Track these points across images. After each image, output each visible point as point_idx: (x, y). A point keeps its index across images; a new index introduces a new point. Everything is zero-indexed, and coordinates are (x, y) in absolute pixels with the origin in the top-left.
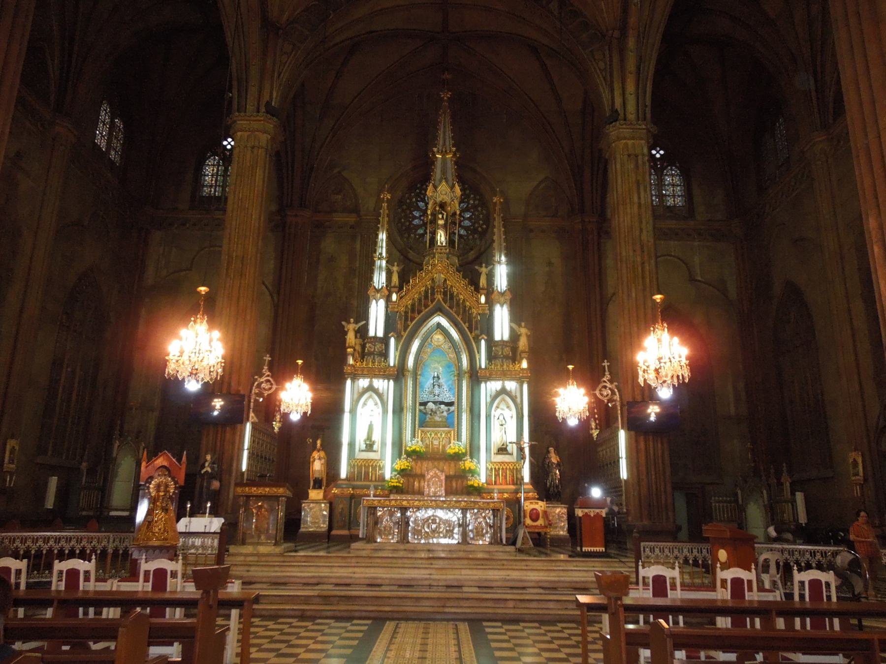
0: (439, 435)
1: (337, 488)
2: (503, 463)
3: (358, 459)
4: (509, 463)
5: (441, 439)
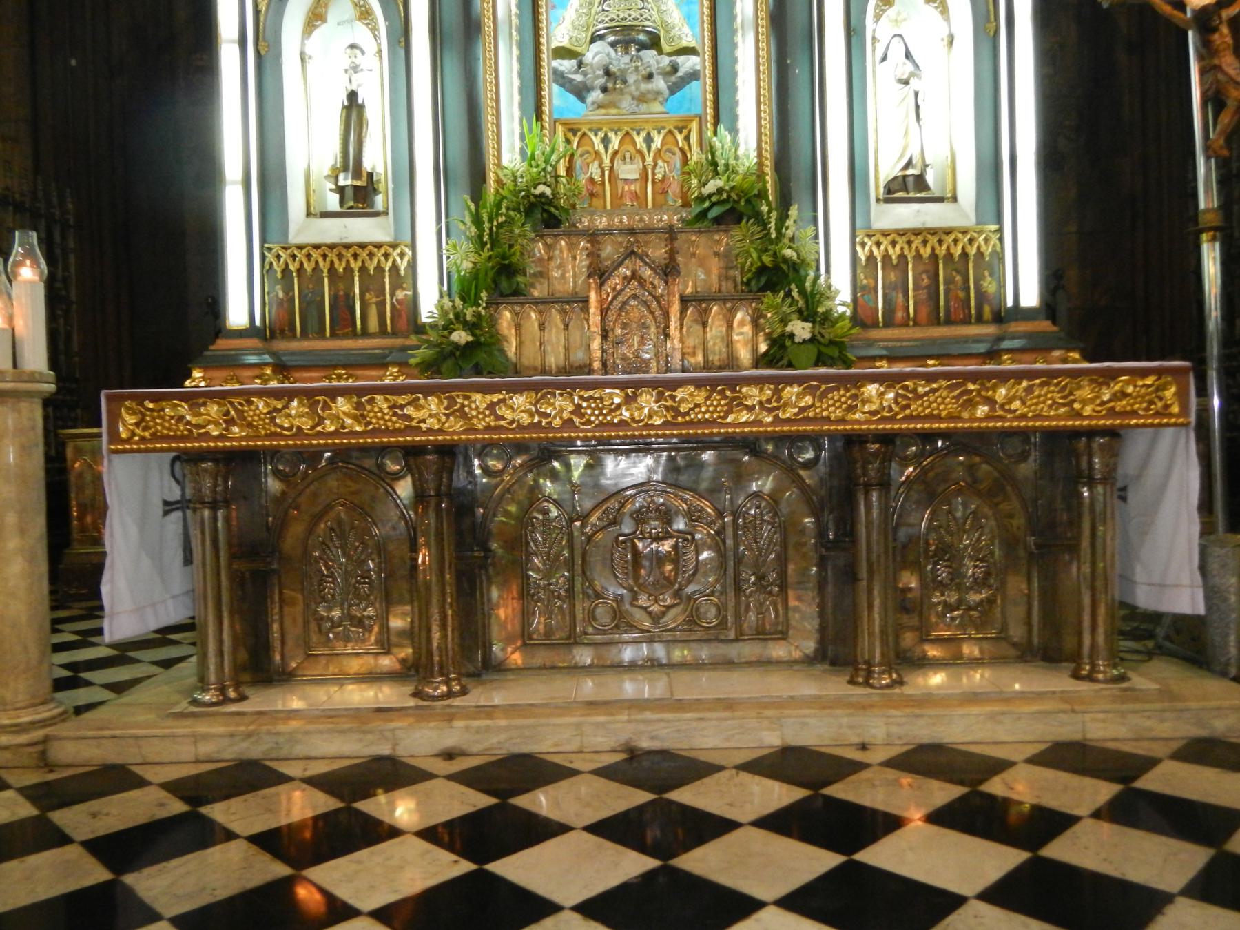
0: (639, 140)
1: (205, 368)
2: (917, 232)
3: (300, 247)
4: (948, 232)
5: (649, 160)
